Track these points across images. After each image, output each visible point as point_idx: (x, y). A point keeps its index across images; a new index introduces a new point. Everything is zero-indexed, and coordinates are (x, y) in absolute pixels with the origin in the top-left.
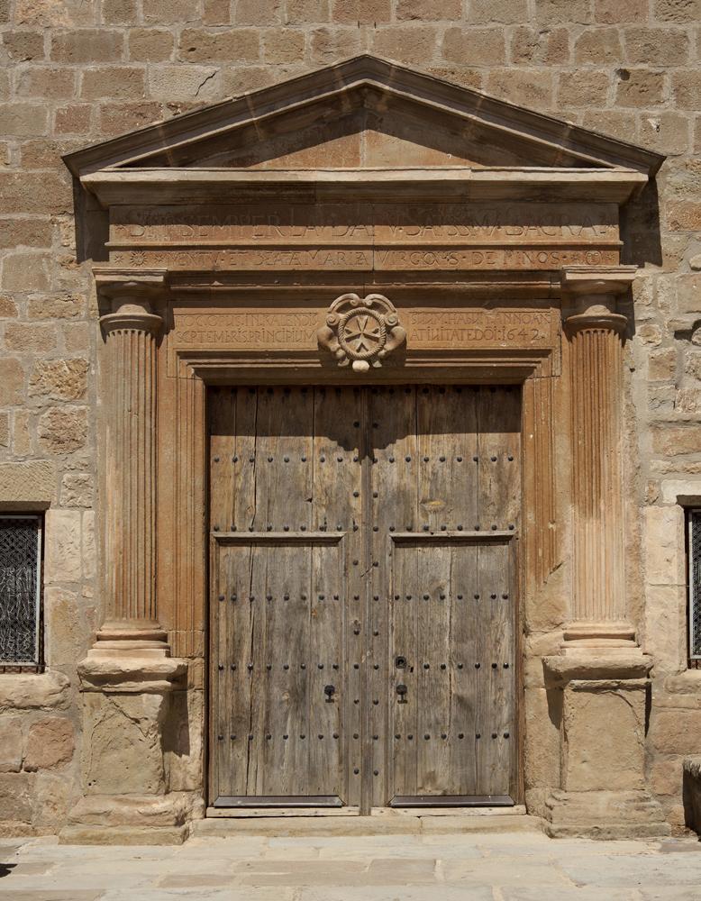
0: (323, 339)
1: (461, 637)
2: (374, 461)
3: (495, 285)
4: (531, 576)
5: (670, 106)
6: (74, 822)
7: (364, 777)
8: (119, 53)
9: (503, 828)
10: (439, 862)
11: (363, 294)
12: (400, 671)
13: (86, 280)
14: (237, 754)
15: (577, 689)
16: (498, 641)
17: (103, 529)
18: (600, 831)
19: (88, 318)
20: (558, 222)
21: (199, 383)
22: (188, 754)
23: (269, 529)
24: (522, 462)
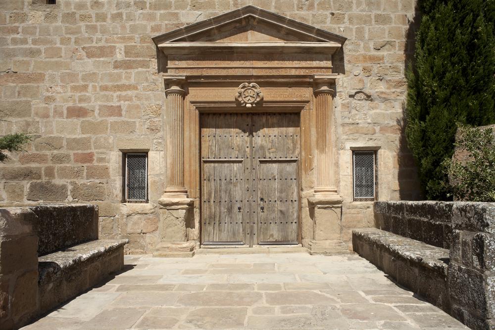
0: (237, 97)
1: (281, 192)
2: (253, 136)
3: (292, 80)
4: (303, 172)
5: (347, 24)
6: (158, 250)
7: (251, 235)
8: (171, 7)
9: (295, 252)
10: (276, 264)
11: (249, 83)
13: (160, 79)
14: (210, 228)
15: (319, 208)
16: (293, 193)
17: (166, 157)
18: (326, 253)
19: (162, 91)
20: (312, 60)
21: (197, 111)
22: (194, 228)
23: (220, 158)
24: (300, 137)
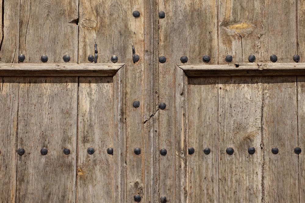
23: (21, 60)
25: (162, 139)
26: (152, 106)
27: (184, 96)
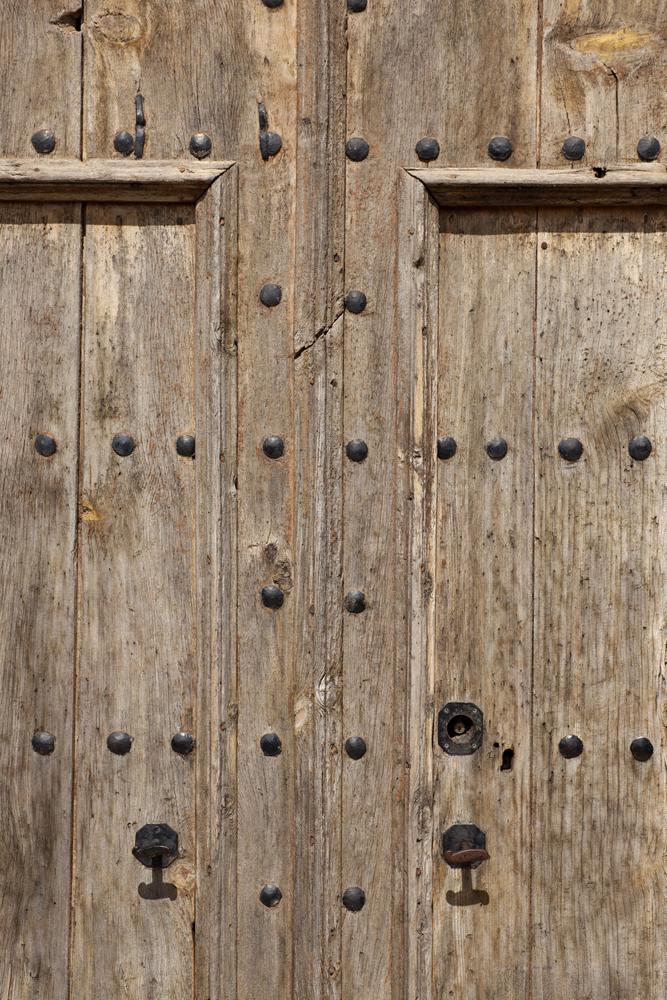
12: (457, 765)
25: (353, 409)
26: (322, 301)
27: (427, 271)
